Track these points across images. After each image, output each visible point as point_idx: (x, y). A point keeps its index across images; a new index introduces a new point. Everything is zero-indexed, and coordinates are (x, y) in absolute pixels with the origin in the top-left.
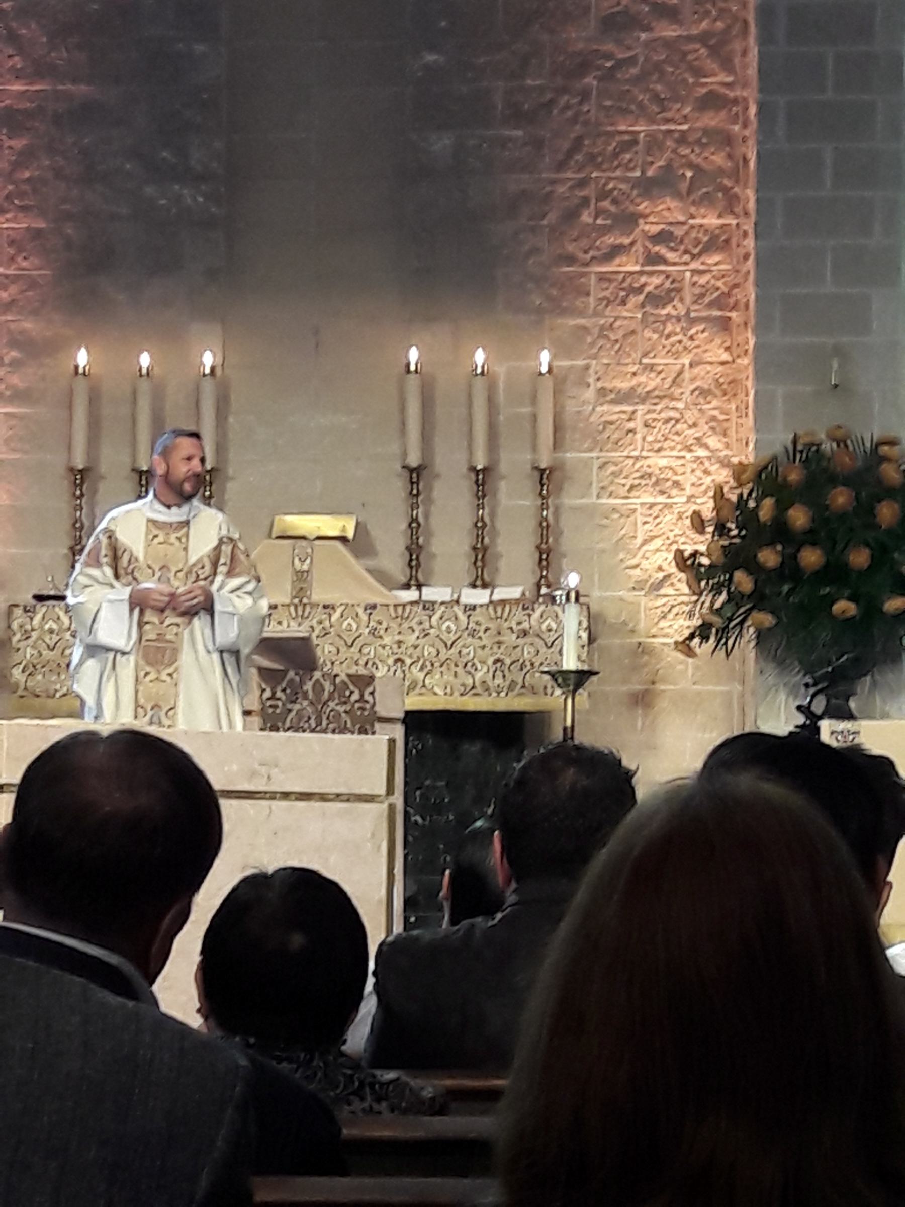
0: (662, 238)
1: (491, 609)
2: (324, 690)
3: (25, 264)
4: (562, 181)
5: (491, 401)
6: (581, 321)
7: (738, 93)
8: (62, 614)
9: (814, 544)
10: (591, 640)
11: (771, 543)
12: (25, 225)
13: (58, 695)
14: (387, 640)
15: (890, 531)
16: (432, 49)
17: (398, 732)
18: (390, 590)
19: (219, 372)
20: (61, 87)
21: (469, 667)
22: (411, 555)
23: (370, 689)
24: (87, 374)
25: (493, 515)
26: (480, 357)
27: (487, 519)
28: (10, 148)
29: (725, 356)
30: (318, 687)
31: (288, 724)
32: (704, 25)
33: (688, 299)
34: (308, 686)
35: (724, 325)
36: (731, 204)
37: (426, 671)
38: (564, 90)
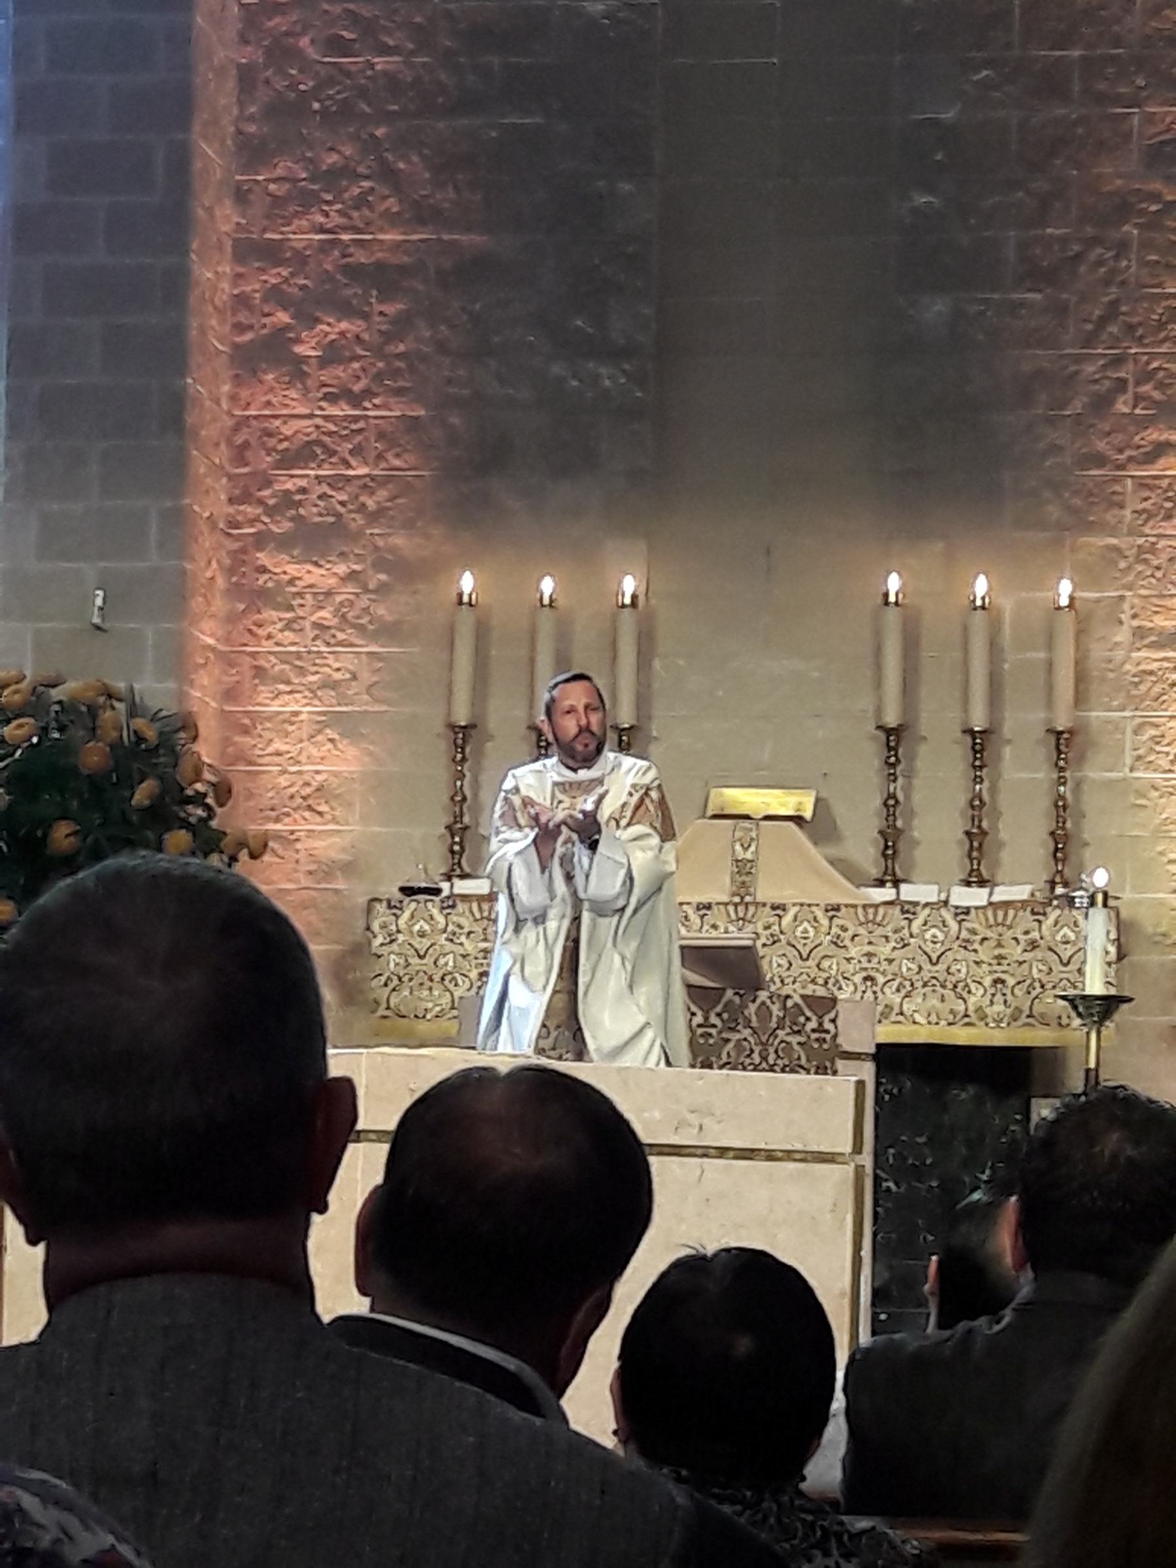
1: (990, 913)
2: (771, 1015)
3: (397, 463)
6: (1114, 541)
8: (435, 912)
10: (1121, 957)
12: (398, 413)
13: (429, 1016)
14: (854, 952)
17: (867, 1071)
18: (858, 887)
19: (641, 600)
20: (446, 237)
21: (960, 990)
22: (886, 841)
23: (832, 1015)
24: (473, 602)
25: (993, 790)
26: (981, 586)
27: (986, 797)
28: (381, 313)
31: (724, 1058)
34: (753, 1008)
37: (903, 992)
38: (1095, 241)
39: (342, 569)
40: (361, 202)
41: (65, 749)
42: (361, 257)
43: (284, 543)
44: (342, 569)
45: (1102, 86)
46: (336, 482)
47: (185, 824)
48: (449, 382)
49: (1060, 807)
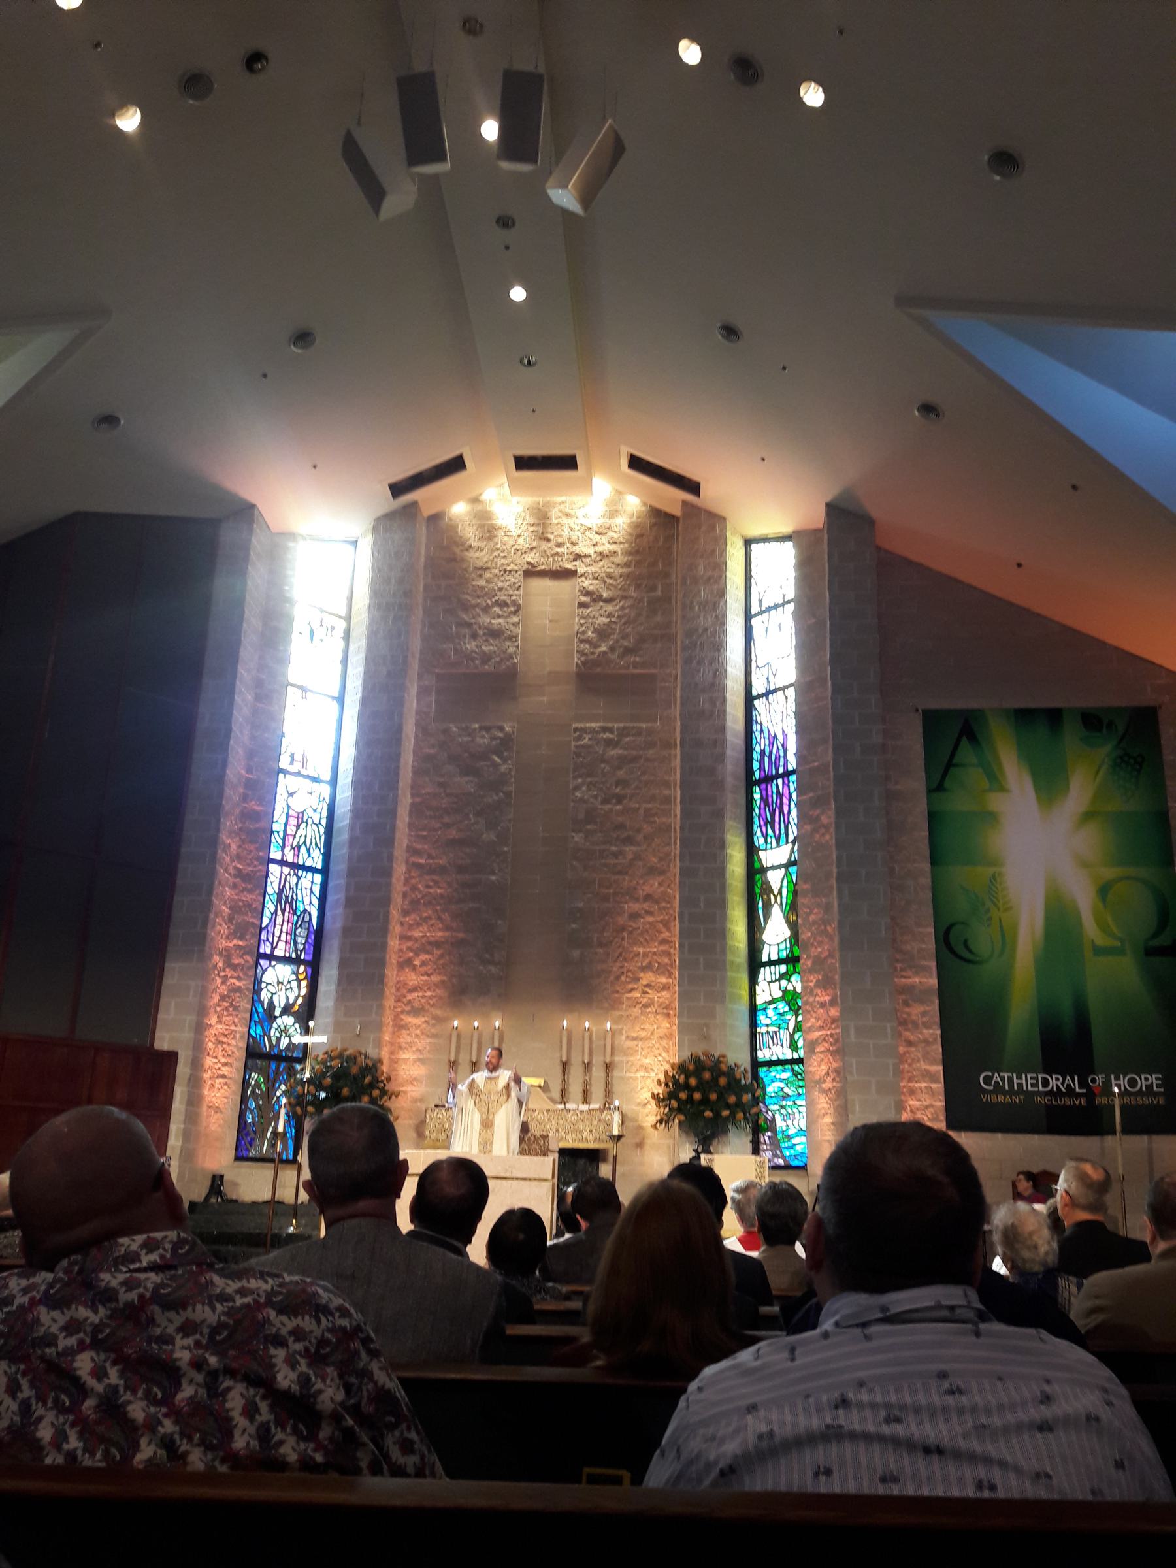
0: (648, 986)
5: (591, 1039)
6: (621, 1013)
7: (672, 939)
8: (443, 1111)
9: (698, 1091)
11: (684, 1091)
15: (724, 1087)
17: (556, 1156)
26: (587, 1025)
30: (529, 1139)
32: (662, 917)
33: (656, 1006)
35: (668, 1015)
36: (670, 975)
38: (615, 938)
39: (423, 1019)
40: (432, 925)
41: (348, 1068)
42: (432, 939)
43: (409, 1013)
44: (423, 1019)
47: (378, 1088)
49: (607, 1084)
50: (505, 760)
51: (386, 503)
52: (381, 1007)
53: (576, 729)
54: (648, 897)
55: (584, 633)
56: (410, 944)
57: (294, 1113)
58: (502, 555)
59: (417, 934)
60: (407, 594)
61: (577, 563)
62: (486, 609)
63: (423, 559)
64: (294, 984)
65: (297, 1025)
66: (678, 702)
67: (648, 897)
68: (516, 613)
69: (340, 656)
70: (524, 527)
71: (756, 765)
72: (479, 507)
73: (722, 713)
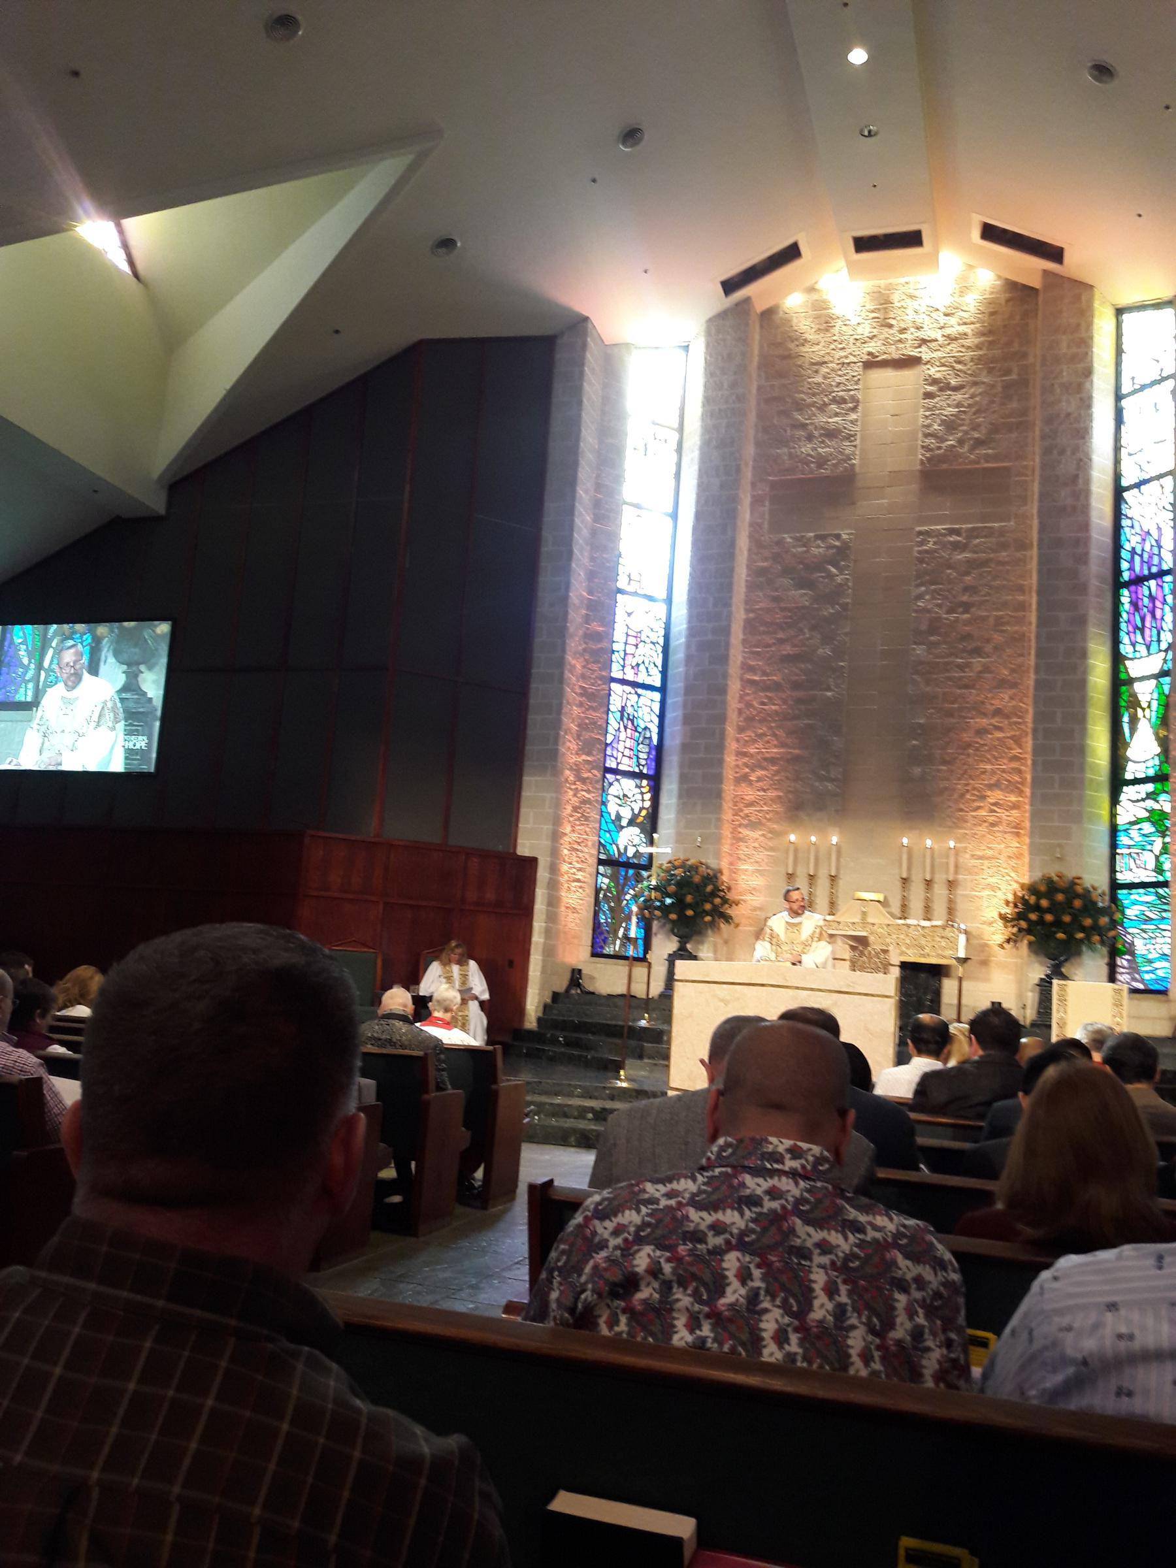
0: (995, 804)
4: (959, 784)
9: (1050, 913)
11: (1033, 912)
14: (894, 936)
15: (1078, 910)
16: (916, 740)
21: (923, 948)
29: (1018, 845)
32: (1013, 733)
35: (1018, 834)
36: (1021, 793)
40: (768, 742)
41: (691, 877)
42: (767, 755)
43: (746, 826)
44: (760, 833)
45: (963, 714)
46: (758, 811)
48: (790, 787)
49: (950, 901)
50: (841, 570)
51: (718, 301)
52: (719, 820)
53: (920, 533)
54: (998, 712)
55: (928, 426)
56: (746, 760)
57: (643, 915)
58: (840, 346)
59: (752, 751)
60: (740, 399)
61: (924, 349)
62: (822, 408)
63: (756, 359)
64: (640, 797)
65: (642, 836)
66: (1036, 497)
67: (998, 712)
68: (854, 409)
69: (674, 470)
70: (864, 314)
71: (1124, 565)
72: (815, 296)
73: (1085, 509)
